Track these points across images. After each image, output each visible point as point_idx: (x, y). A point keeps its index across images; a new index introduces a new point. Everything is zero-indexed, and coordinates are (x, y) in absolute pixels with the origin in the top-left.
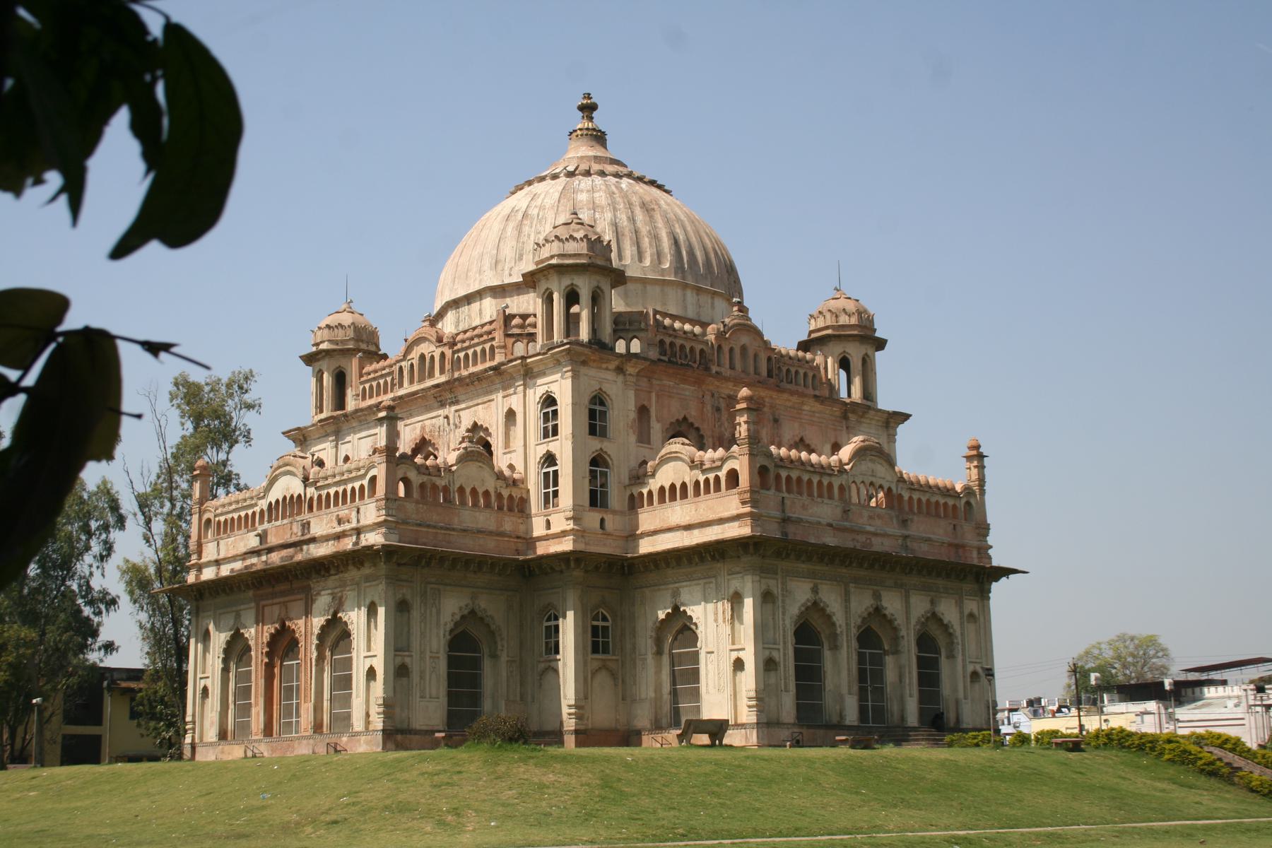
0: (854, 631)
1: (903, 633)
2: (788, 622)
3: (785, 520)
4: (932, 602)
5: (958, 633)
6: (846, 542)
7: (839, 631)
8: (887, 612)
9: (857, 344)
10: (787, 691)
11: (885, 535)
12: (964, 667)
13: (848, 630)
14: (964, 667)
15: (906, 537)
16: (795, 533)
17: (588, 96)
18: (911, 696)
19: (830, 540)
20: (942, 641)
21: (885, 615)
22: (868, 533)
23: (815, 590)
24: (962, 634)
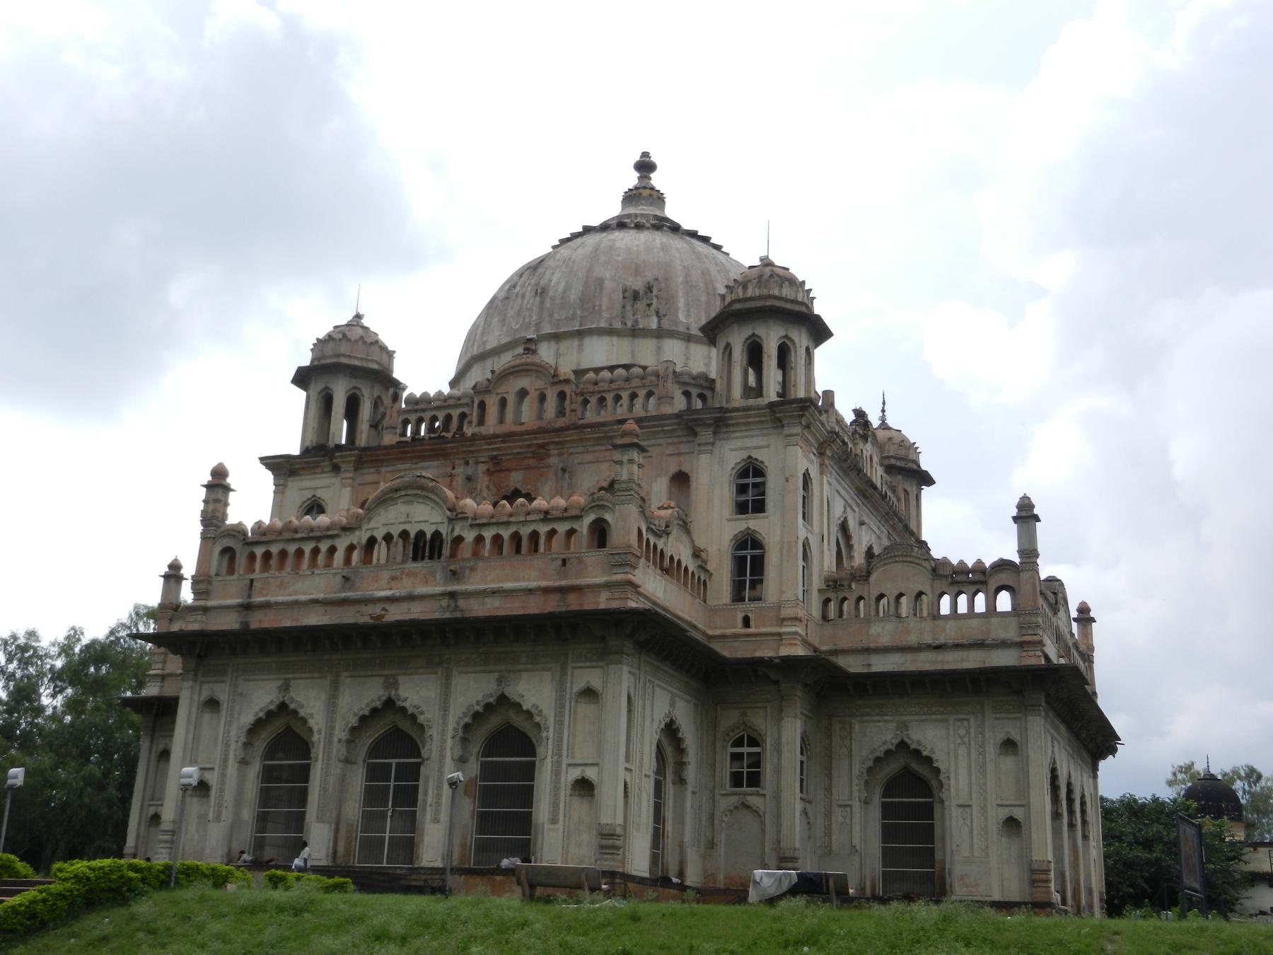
0: (340, 733)
1: (434, 732)
2: (234, 732)
3: (247, 607)
4: (499, 682)
5: (551, 722)
6: (348, 617)
7: (315, 737)
8: (407, 704)
9: (736, 327)
10: (218, 818)
11: (411, 598)
12: (557, 774)
13: (330, 734)
14: (557, 774)
15: (452, 595)
16: (259, 621)
17: (645, 155)
18: (436, 820)
19: (314, 619)
20: (532, 734)
21: (403, 710)
22: (381, 600)
23: (285, 688)
24: (559, 723)
